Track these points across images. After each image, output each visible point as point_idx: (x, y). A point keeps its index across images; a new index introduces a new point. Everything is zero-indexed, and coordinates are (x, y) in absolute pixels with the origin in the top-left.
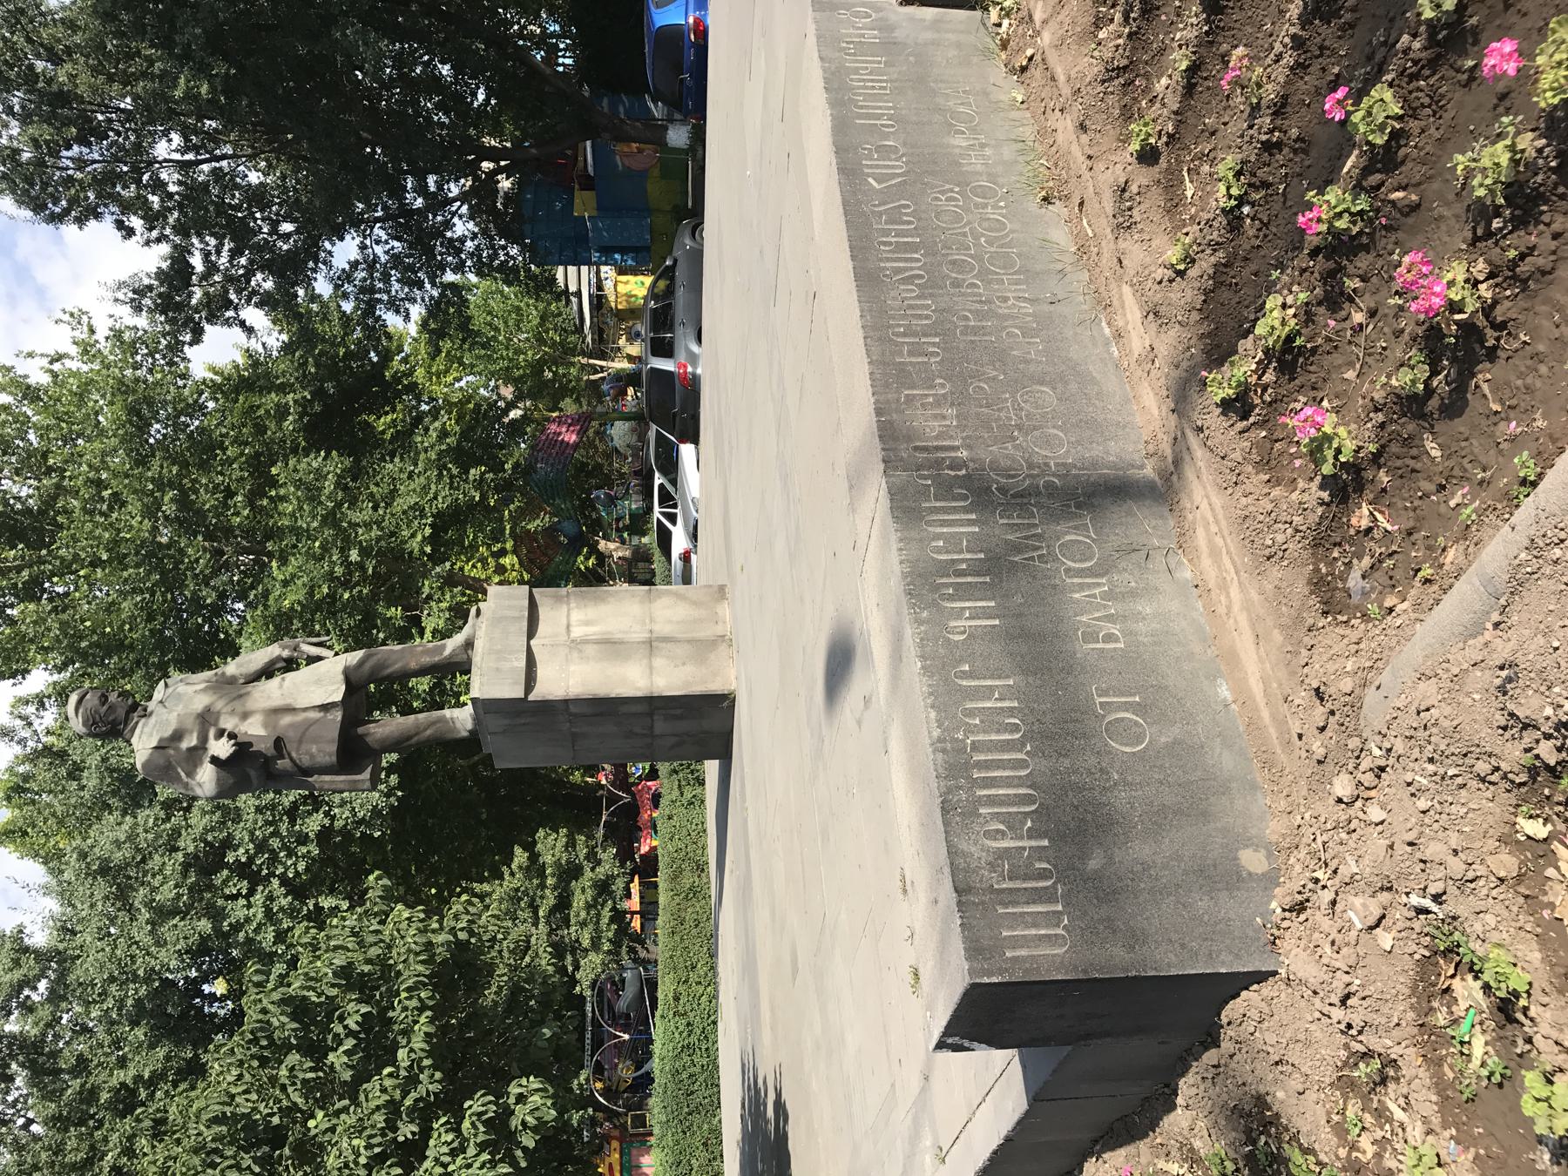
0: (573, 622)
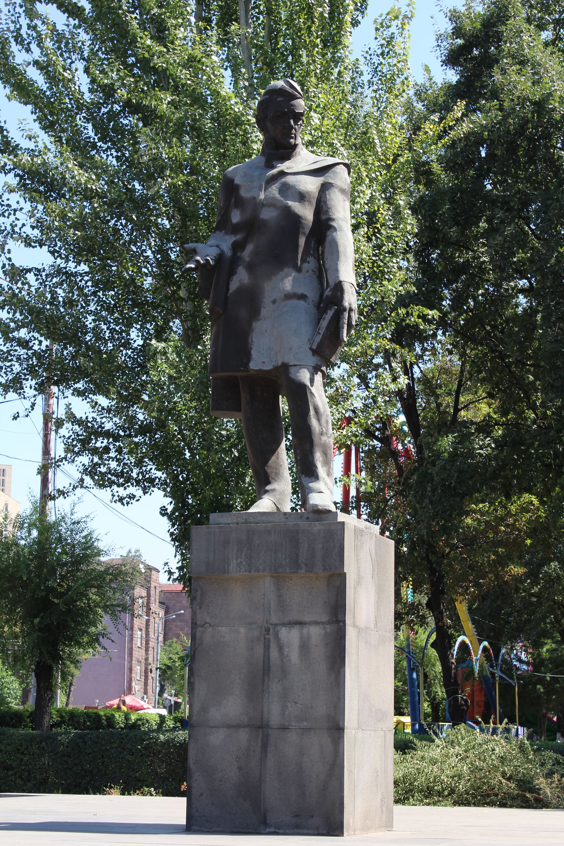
0: (305, 630)
